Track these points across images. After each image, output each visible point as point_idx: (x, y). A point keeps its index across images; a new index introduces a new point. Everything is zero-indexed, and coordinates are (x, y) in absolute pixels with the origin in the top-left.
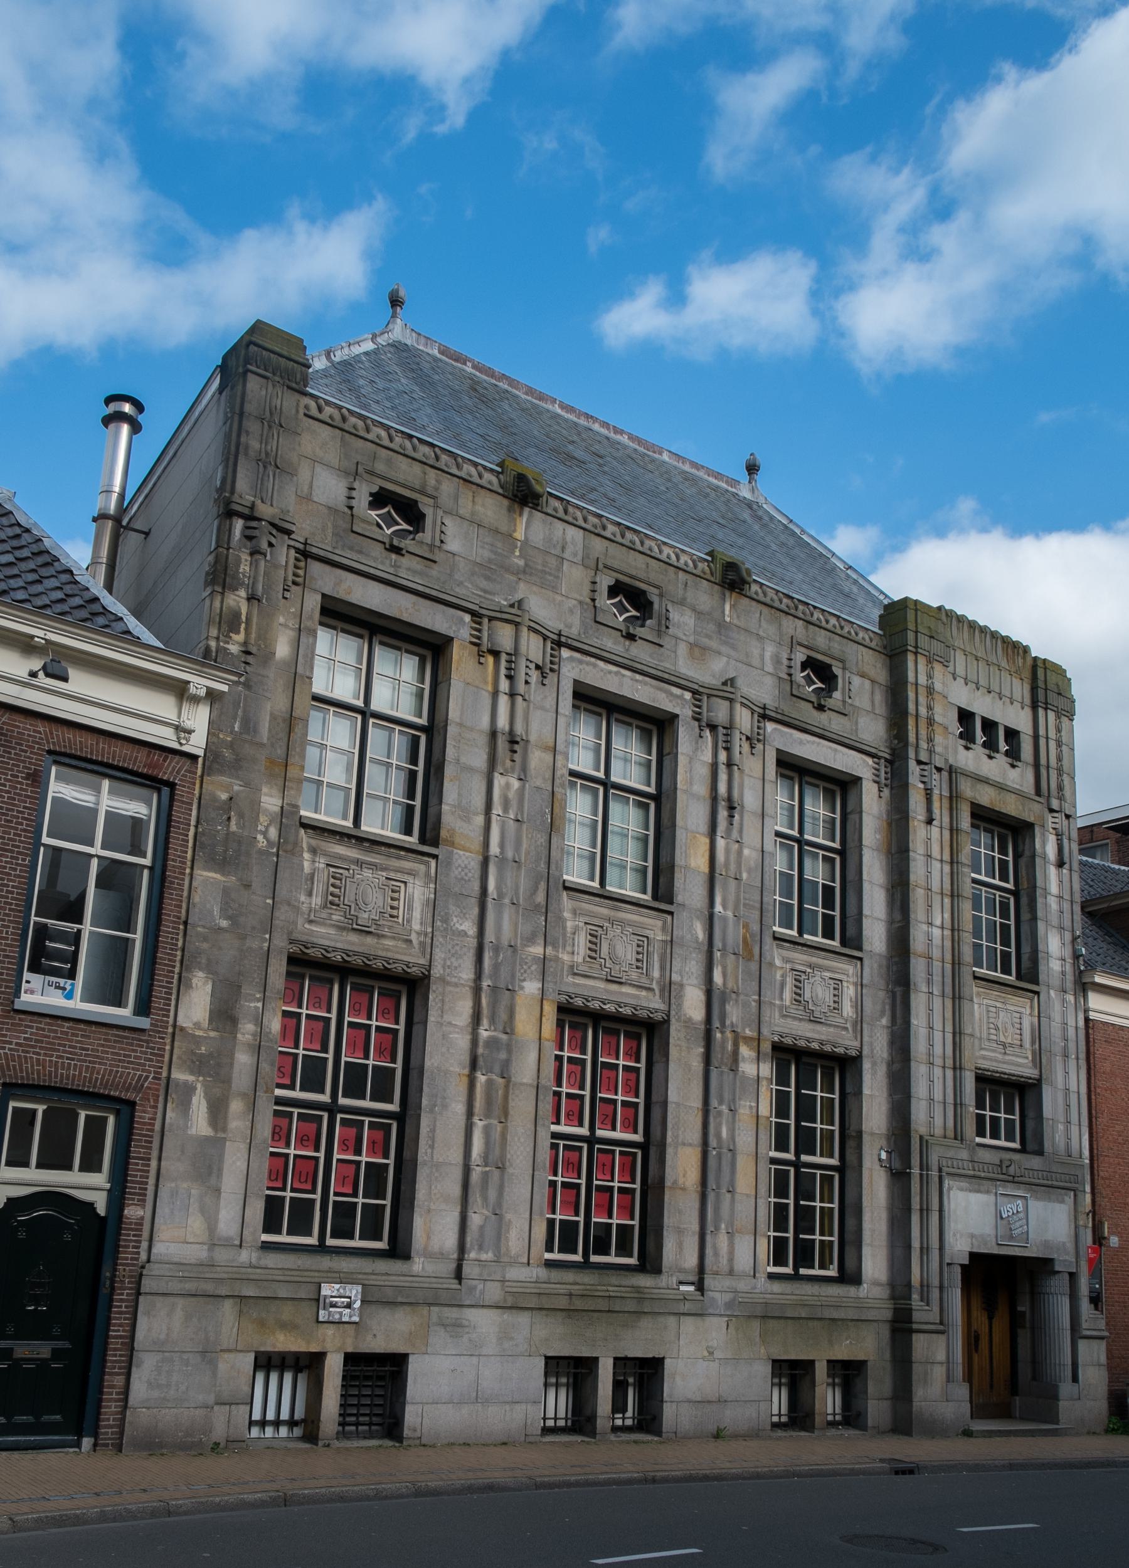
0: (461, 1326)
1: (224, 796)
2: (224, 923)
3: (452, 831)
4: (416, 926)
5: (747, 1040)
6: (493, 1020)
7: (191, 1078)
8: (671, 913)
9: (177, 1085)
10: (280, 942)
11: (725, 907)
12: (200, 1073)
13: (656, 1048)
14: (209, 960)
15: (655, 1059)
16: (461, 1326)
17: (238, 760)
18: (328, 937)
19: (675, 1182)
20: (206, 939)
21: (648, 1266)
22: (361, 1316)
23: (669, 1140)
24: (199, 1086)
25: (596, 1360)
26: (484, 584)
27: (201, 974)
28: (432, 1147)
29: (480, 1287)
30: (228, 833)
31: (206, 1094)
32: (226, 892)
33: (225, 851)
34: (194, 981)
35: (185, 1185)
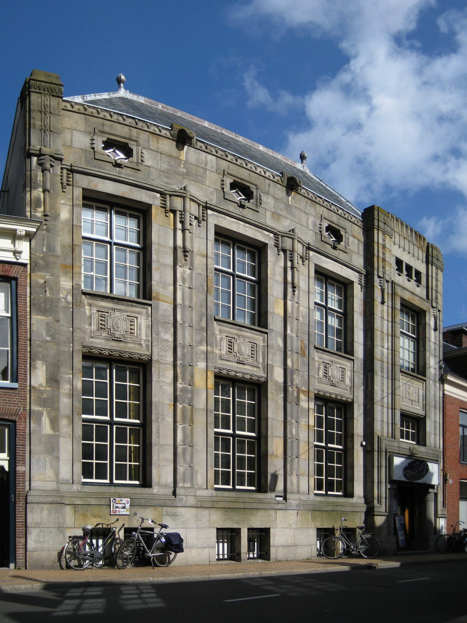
0: (177, 516)
2: (48, 339)
3: (158, 293)
4: (143, 337)
5: (303, 392)
6: (183, 379)
7: (41, 409)
8: (267, 333)
9: (34, 412)
10: (78, 347)
11: (292, 331)
14: (43, 356)
16: (177, 516)
18: (100, 343)
20: (40, 346)
24: (44, 412)
27: (40, 362)
30: (46, 298)
31: (48, 416)
32: (48, 324)
33: (46, 306)
34: (37, 365)
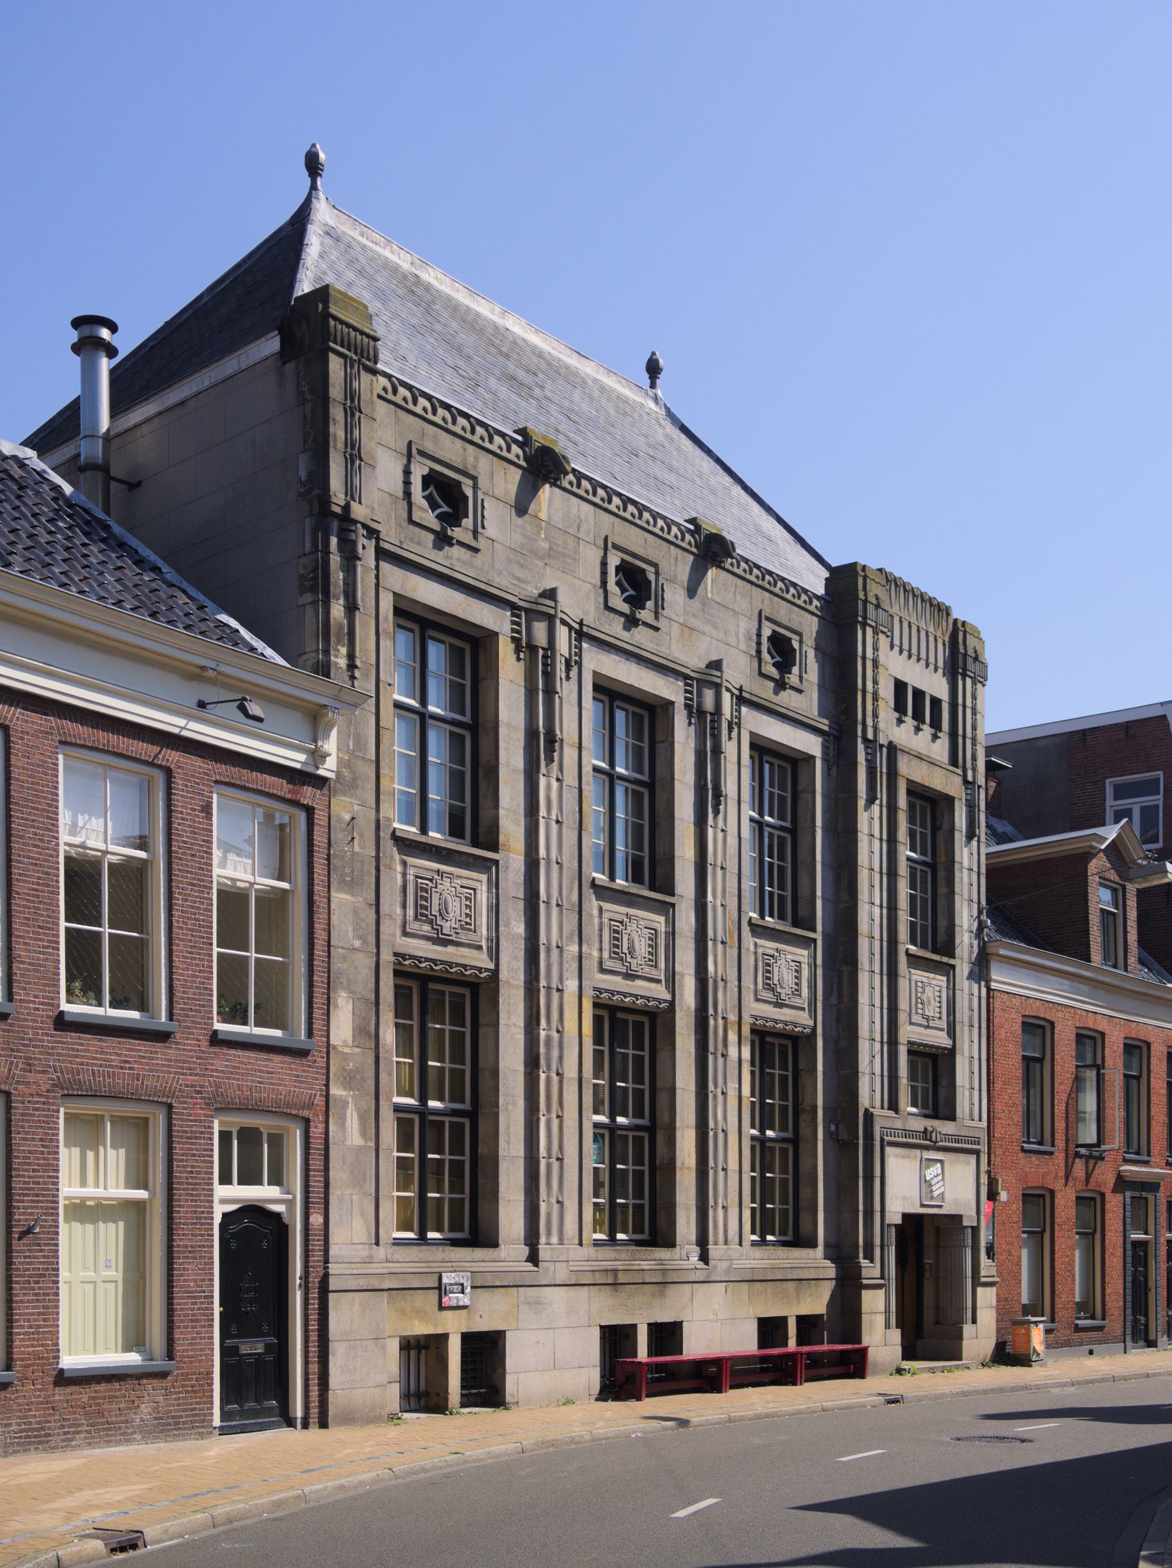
0: (540, 1303)
1: (347, 817)
2: (357, 943)
7: (344, 1093)
9: (335, 1100)
12: (351, 1089)
13: (659, 1036)
14: (349, 980)
15: (658, 1047)
16: (540, 1303)
17: (355, 779)
19: (683, 1163)
20: (345, 960)
21: (659, 1241)
22: (471, 1299)
23: (678, 1124)
25: (634, 1326)
26: (519, 572)
27: (344, 994)
28: (508, 1143)
29: (552, 1268)
30: (353, 853)
31: (356, 1105)
33: (352, 872)
34: (340, 1001)
35: (348, 1192)
